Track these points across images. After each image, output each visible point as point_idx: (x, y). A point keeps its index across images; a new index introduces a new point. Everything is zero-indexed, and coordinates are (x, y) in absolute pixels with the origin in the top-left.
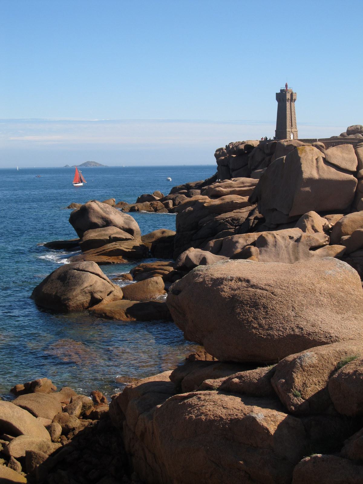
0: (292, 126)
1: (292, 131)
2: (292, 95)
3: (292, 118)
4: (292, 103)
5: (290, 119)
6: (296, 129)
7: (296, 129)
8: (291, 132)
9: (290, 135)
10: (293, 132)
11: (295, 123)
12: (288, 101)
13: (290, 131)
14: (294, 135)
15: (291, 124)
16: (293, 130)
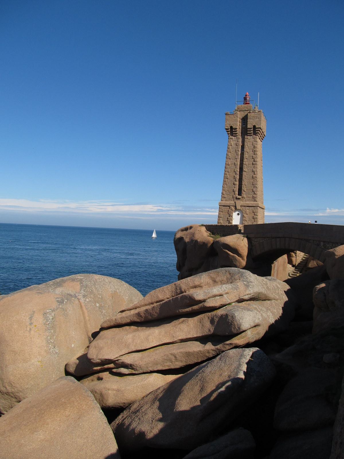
0: (240, 193)
1: (235, 207)
2: (245, 120)
3: (244, 174)
4: (249, 139)
5: (238, 177)
6: (255, 201)
7: (255, 201)
8: (233, 208)
9: (231, 216)
10: (238, 207)
11: (254, 185)
12: (232, 135)
13: (229, 206)
14: (243, 217)
15: (237, 189)
16: (239, 203)
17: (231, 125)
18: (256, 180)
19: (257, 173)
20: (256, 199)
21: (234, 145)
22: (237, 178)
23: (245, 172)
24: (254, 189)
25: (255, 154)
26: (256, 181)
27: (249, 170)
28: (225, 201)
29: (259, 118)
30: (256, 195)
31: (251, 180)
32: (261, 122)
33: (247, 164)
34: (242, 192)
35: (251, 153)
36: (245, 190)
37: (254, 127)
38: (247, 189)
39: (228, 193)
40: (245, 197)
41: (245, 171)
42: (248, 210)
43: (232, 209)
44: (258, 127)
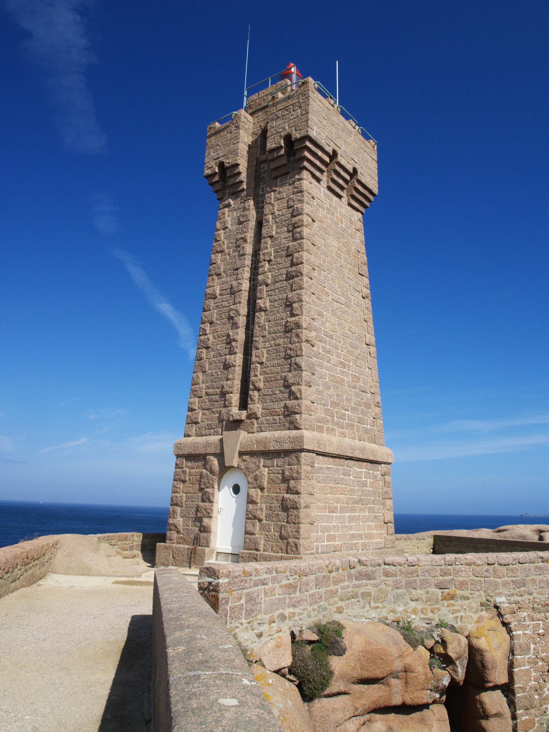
6: (297, 428)
11: (291, 359)
17: (221, 159)
18: (298, 336)
19: (301, 307)
20: (298, 416)
21: (232, 225)
22: (234, 340)
23: (263, 313)
24: (290, 376)
25: (298, 235)
26: (296, 340)
27: (275, 301)
28: (198, 435)
29: (300, 107)
30: (296, 398)
31: (281, 341)
32: (310, 116)
33: (269, 281)
34: (251, 393)
35: (284, 238)
36: (261, 385)
37: (288, 138)
38: (266, 381)
39: (208, 404)
40: (259, 415)
41: (261, 310)
42: (265, 471)
43: (211, 468)
44: (298, 136)
